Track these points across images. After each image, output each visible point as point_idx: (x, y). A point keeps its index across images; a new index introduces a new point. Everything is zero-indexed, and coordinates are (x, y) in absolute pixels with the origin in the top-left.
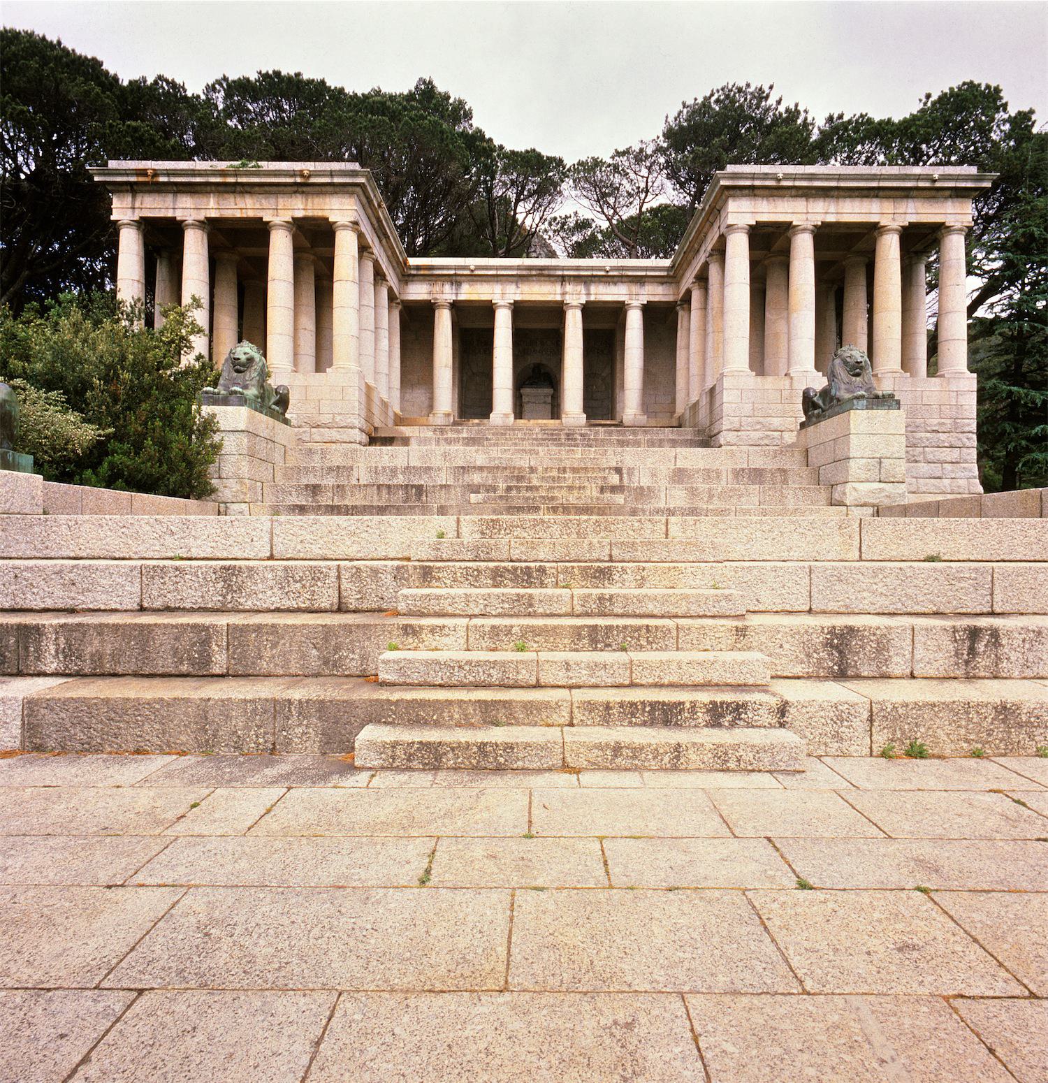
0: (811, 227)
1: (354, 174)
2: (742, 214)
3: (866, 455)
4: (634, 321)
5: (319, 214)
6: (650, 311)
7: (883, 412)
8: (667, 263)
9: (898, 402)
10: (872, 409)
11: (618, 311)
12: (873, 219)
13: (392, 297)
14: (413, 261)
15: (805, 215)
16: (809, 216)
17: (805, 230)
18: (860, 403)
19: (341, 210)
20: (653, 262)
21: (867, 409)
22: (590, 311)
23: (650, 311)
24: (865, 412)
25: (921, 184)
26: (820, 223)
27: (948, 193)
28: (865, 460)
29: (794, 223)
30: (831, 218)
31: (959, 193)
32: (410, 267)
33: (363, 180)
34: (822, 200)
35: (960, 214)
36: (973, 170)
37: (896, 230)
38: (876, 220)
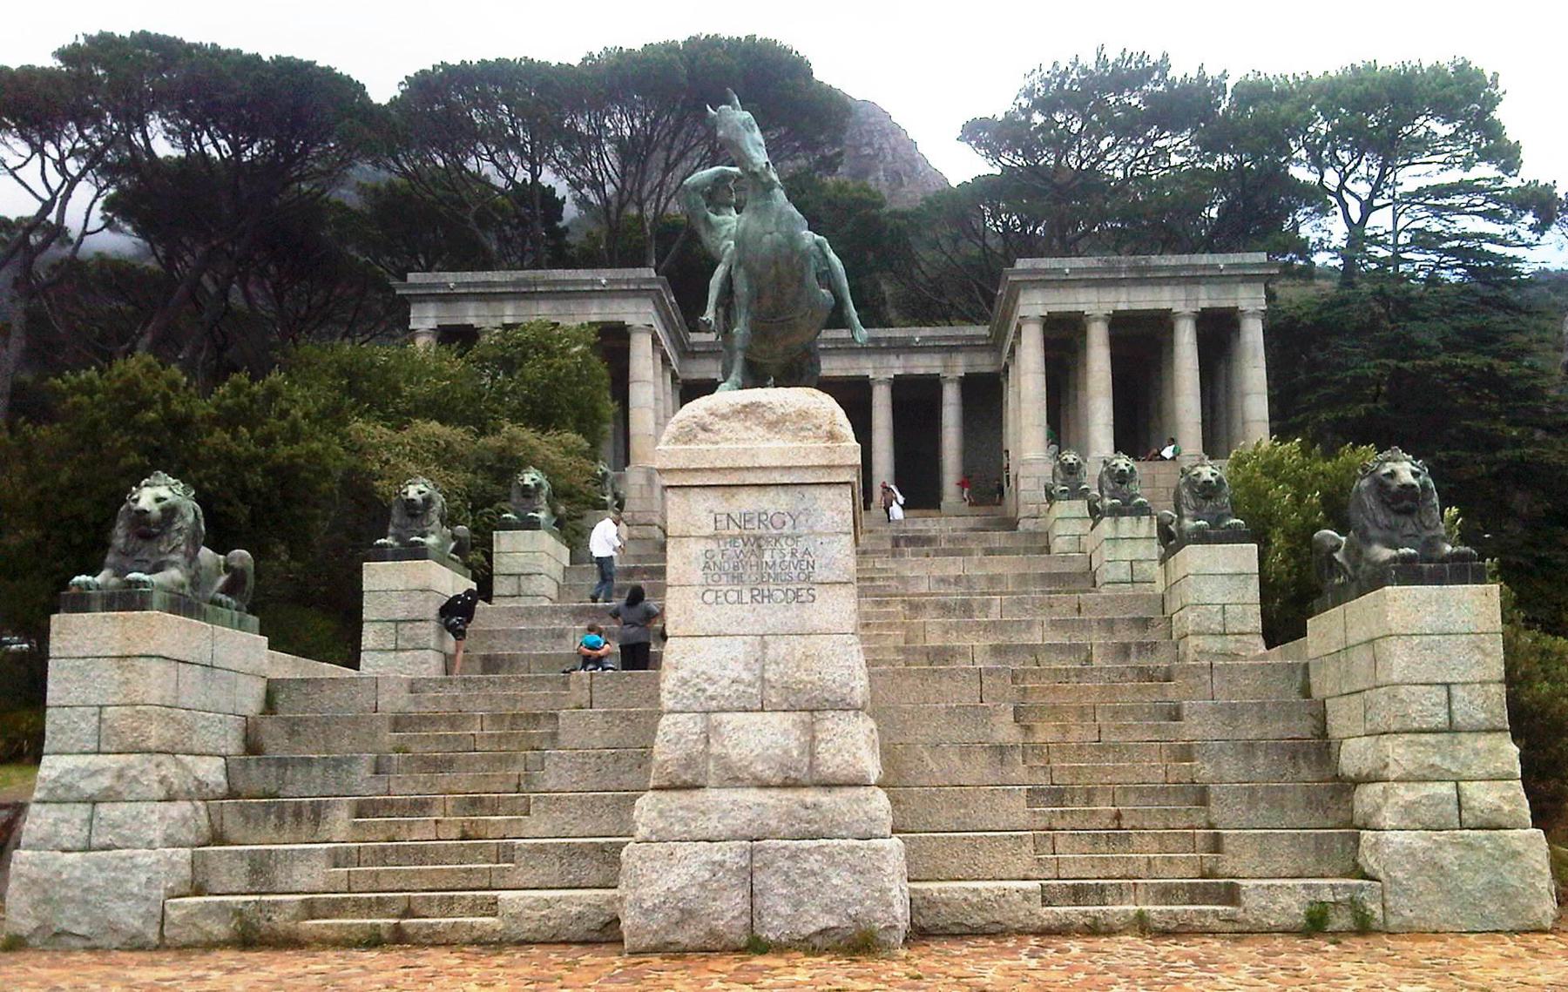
1: (650, 281)
2: (1034, 305)
4: (951, 395)
5: (615, 318)
6: (970, 385)
8: (983, 330)
11: (933, 385)
12: (1164, 306)
13: (674, 377)
14: (695, 337)
15: (1097, 304)
17: (1096, 319)
19: (638, 315)
20: (970, 330)
22: (900, 385)
23: (970, 385)
25: (1208, 273)
30: (1121, 307)
31: (1248, 279)
32: (694, 344)
33: (659, 287)
35: (1250, 300)
36: (1263, 257)
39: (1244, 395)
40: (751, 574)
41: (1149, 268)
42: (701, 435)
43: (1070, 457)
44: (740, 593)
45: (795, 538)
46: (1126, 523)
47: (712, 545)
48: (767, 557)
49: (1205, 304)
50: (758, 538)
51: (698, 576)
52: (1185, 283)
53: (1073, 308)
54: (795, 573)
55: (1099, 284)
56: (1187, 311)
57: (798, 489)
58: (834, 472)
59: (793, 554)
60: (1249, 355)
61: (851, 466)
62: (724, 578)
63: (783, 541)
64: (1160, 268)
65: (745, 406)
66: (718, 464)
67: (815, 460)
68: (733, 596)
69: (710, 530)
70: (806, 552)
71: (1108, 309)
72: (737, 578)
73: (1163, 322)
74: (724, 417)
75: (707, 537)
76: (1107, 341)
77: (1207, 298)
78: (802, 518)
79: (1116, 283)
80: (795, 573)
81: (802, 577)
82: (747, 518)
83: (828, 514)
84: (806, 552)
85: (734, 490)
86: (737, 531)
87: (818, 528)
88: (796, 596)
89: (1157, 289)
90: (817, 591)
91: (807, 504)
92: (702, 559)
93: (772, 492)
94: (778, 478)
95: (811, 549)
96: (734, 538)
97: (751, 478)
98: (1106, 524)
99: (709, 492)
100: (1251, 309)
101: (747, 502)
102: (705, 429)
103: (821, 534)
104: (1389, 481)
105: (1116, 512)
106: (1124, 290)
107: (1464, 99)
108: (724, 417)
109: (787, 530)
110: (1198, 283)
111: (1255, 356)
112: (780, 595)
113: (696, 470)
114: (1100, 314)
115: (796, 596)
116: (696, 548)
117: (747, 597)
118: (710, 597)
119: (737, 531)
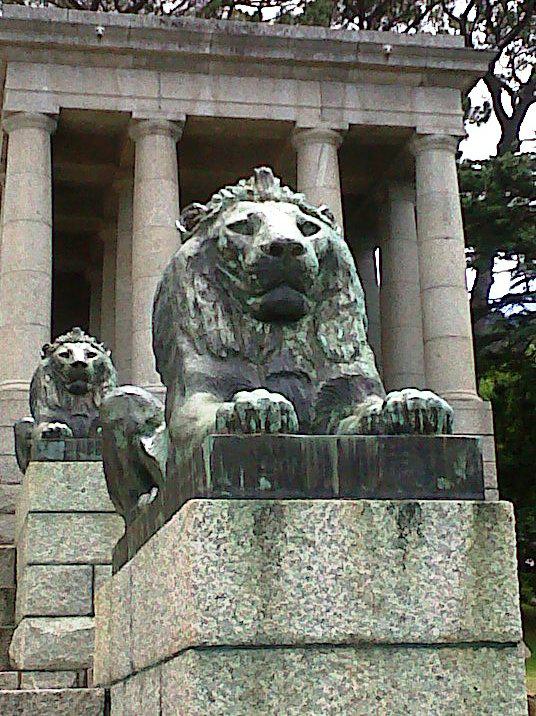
3: (62, 557)
12: (288, 115)
17: (155, 129)
18: (53, 445)
27: (418, 77)
28: (57, 569)
30: (204, 110)
34: (187, 76)
37: (328, 136)
38: (291, 118)
39: (425, 290)
43: (79, 348)
46: (328, 532)
49: (356, 118)
52: (319, 79)
53: (108, 104)
55: (159, 63)
56: (324, 127)
60: (437, 214)
71: (178, 111)
77: (358, 108)
79: (192, 65)
89: (268, 83)
98: (197, 541)
100: (439, 133)
105: (264, 468)
110: (344, 80)
111: (446, 219)
114: (162, 119)
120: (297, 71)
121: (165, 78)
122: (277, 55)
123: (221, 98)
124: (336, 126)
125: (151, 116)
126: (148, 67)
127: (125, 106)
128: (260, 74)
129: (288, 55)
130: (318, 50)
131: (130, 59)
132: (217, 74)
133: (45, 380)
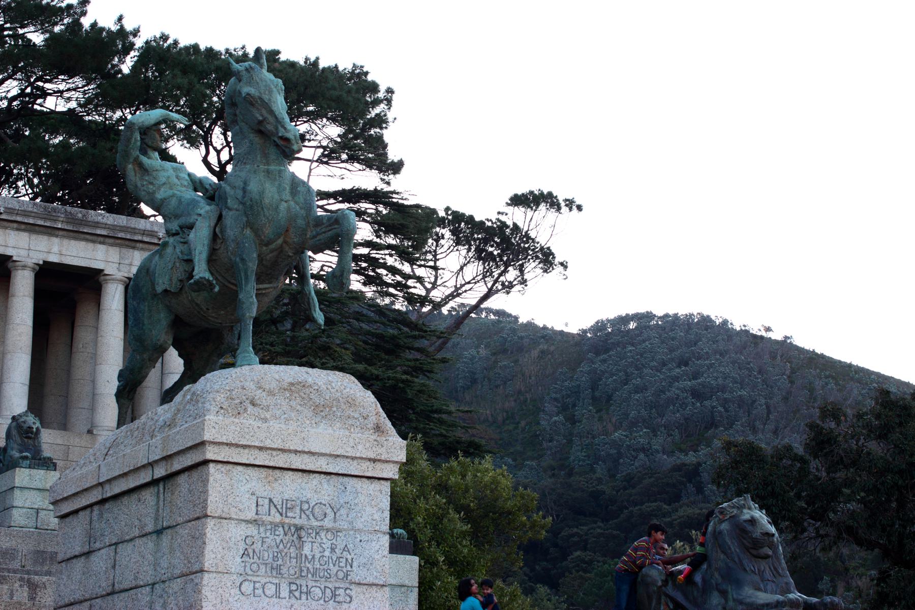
0: (31, 265)
3: (26, 505)
7: (42, 472)
9: (55, 465)
10: (34, 468)
16: (32, 254)
17: (24, 267)
18: (25, 462)
21: (30, 467)
24: (28, 470)
26: (41, 262)
28: (25, 510)
29: (14, 258)
34: (46, 238)
40: (290, 567)
41: (84, 222)
42: (250, 408)
44: (278, 586)
45: (336, 532)
47: (252, 530)
48: (307, 550)
50: (299, 528)
51: (235, 563)
52: (120, 246)
54: (334, 570)
55: (32, 229)
56: (120, 275)
57: (341, 479)
58: (379, 465)
59: (333, 550)
61: (396, 462)
62: (263, 567)
63: (323, 534)
64: (97, 225)
65: (292, 384)
66: (268, 443)
67: (361, 451)
68: (271, 590)
69: (250, 515)
70: (345, 549)
72: (277, 570)
73: (89, 282)
74: (271, 393)
75: (247, 522)
76: (32, 294)
78: (343, 511)
79: (50, 231)
80: (334, 570)
81: (341, 575)
82: (287, 507)
83: (368, 509)
84: (345, 549)
85: (277, 472)
86: (278, 518)
87: (359, 525)
88: (334, 595)
89: (91, 245)
90: (355, 591)
91: (348, 497)
92: (242, 546)
93: (315, 480)
94: (322, 464)
95: (350, 546)
96: (275, 526)
97: (298, 462)
99: (250, 471)
101: (290, 487)
102: (253, 404)
103: (359, 531)
104: (749, 528)
106: (56, 240)
107: (348, 101)
108: (271, 393)
109: (328, 523)
110: (134, 248)
112: (317, 592)
113: (244, 447)
115: (334, 595)
116: (237, 532)
117: (285, 593)
118: (247, 587)
119: (278, 518)
120: (107, 240)
121: (34, 237)
122: (99, 232)
123: (64, 252)
124: (126, 275)
125: (23, 259)
126: (24, 230)
127: (9, 252)
128: (87, 240)
129: (104, 232)
130: (121, 231)
131: (15, 225)
132: (63, 237)
133: (14, 432)
